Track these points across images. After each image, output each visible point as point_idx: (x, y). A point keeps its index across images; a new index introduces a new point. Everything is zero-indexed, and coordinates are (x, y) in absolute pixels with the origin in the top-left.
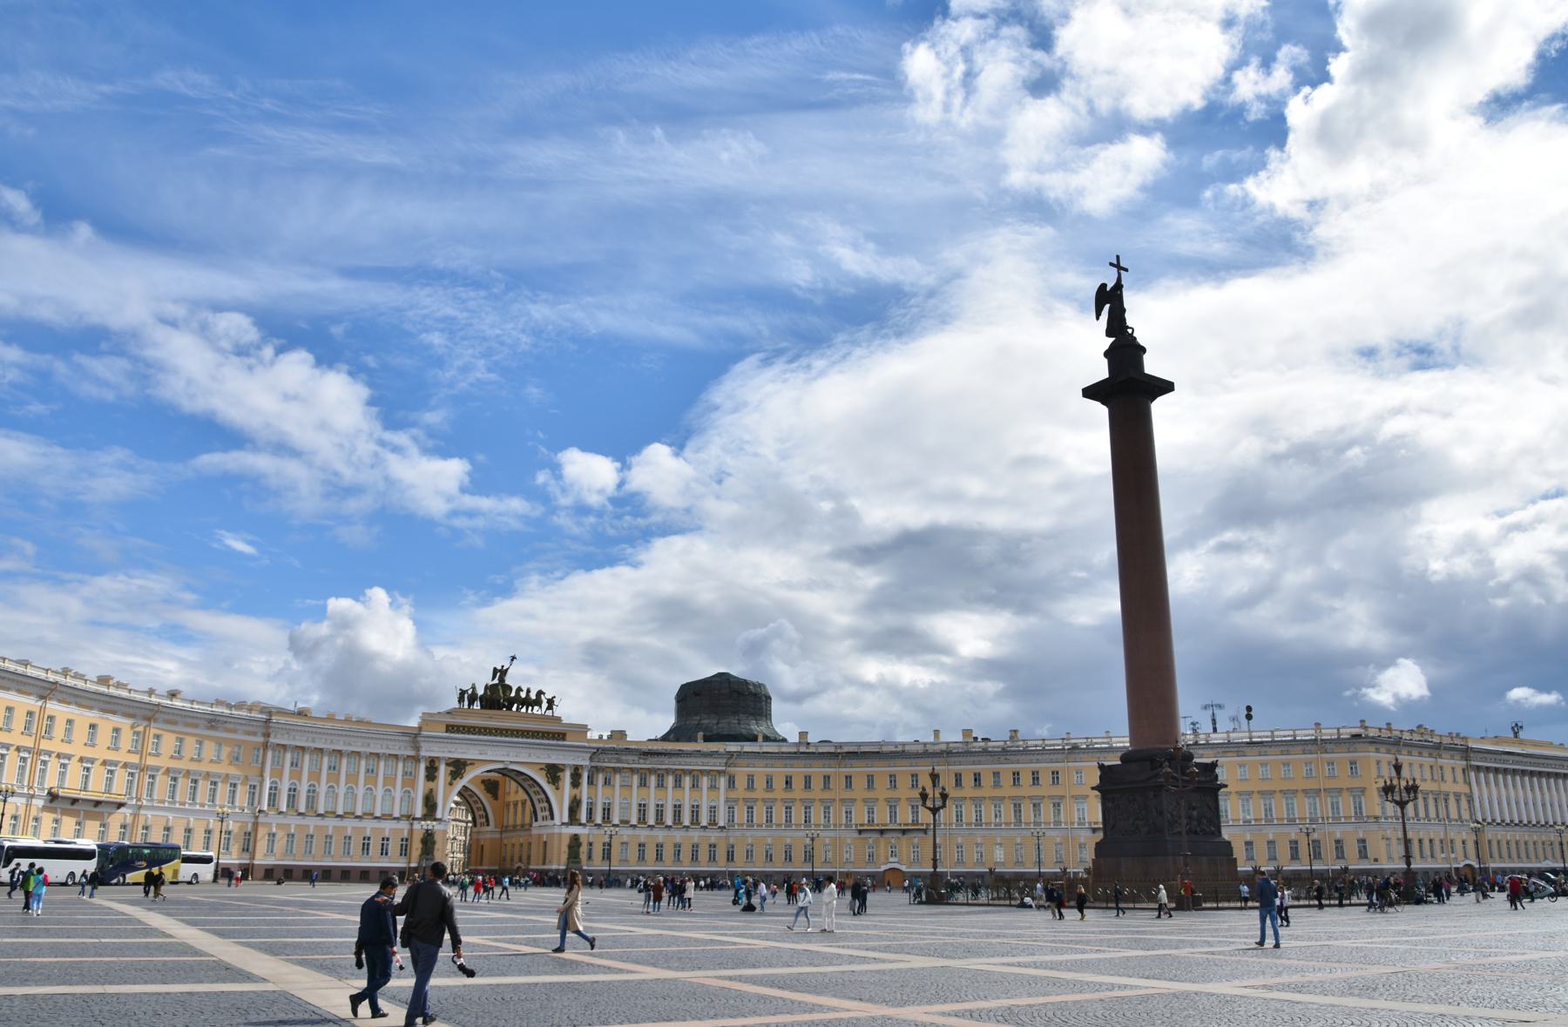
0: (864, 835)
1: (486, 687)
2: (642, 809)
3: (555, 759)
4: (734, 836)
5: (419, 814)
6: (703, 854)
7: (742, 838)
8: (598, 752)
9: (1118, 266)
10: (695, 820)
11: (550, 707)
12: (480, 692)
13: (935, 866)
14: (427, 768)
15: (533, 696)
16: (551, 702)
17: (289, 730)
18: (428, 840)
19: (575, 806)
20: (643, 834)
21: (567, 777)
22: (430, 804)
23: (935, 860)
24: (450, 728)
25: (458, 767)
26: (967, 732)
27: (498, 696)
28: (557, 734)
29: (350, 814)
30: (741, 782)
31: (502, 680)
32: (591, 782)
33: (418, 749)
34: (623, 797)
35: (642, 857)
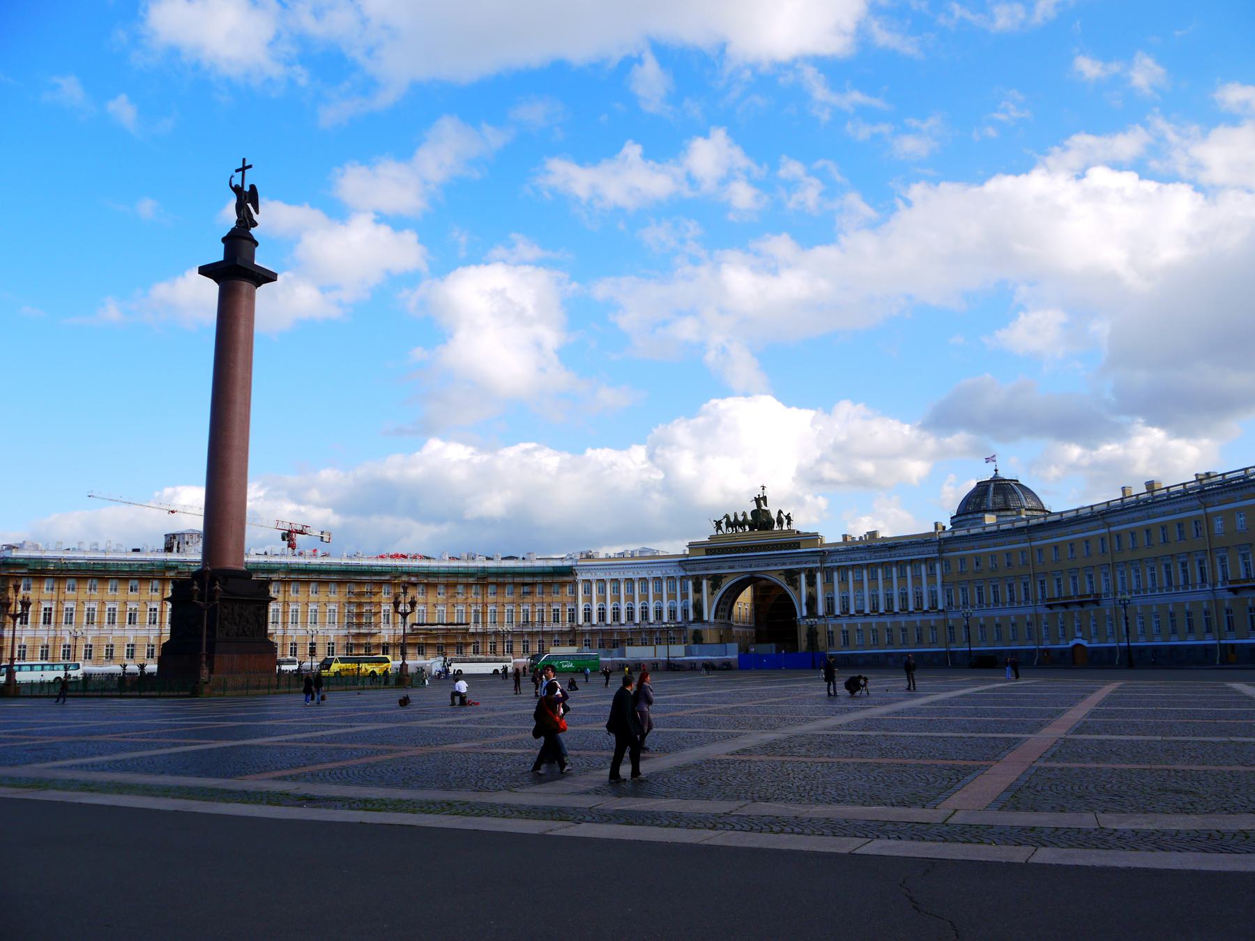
0: (1056, 610)
1: (753, 513)
4: (953, 617)
8: (826, 554)
10: (919, 607)
11: (789, 523)
16: (788, 517)
24: (709, 551)
26: (1150, 485)
28: (796, 541)
30: (956, 566)
32: (829, 581)
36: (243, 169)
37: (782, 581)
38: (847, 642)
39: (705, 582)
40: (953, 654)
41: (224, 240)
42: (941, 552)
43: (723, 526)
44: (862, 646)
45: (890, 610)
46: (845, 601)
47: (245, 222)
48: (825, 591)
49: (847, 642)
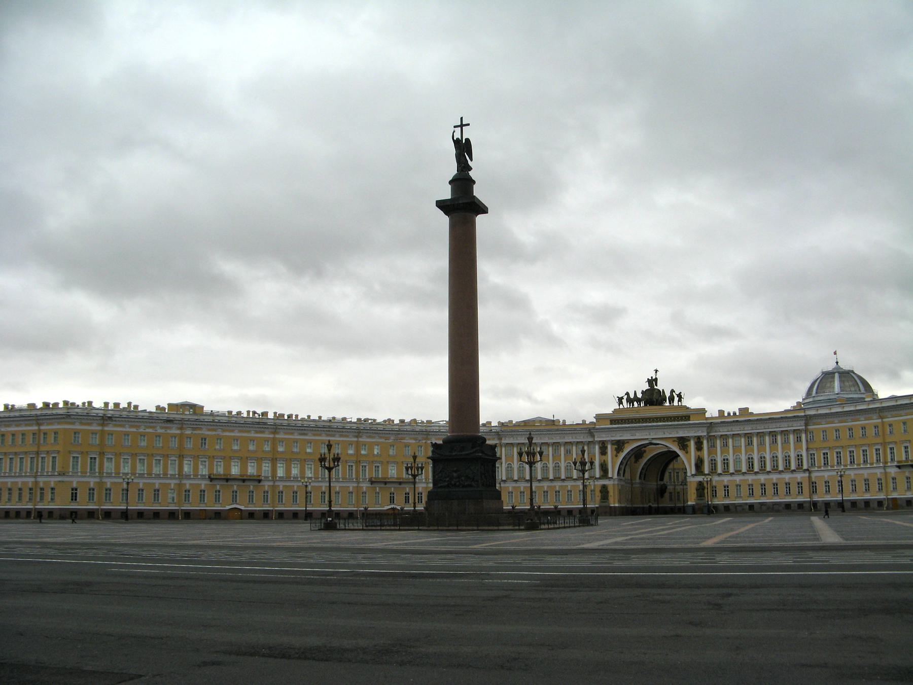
0: (903, 470)
3: (681, 434)
5: (598, 476)
6: (794, 489)
7: (822, 475)
8: (711, 425)
11: (680, 400)
12: (639, 395)
13: (330, 506)
14: (600, 448)
15: (668, 394)
16: (679, 396)
18: (604, 490)
20: (750, 478)
21: (692, 444)
22: (604, 468)
23: (330, 502)
24: (613, 421)
27: (653, 396)
28: (685, 416)
29: (557, 479)
33: (593, 436)
34: (736, 454)
35: (752, 494)
36: (462, 126)
37: (675, 448)
38: (727, 495)
39: (609, 447)
40: (815, 504)
41: (450, 182)
42: (806, 425)
43: (624, 401)
44: (739, 496)
45: (763, 469)
46: (726, 462)
48: (709, 453)
49: (727, 495)
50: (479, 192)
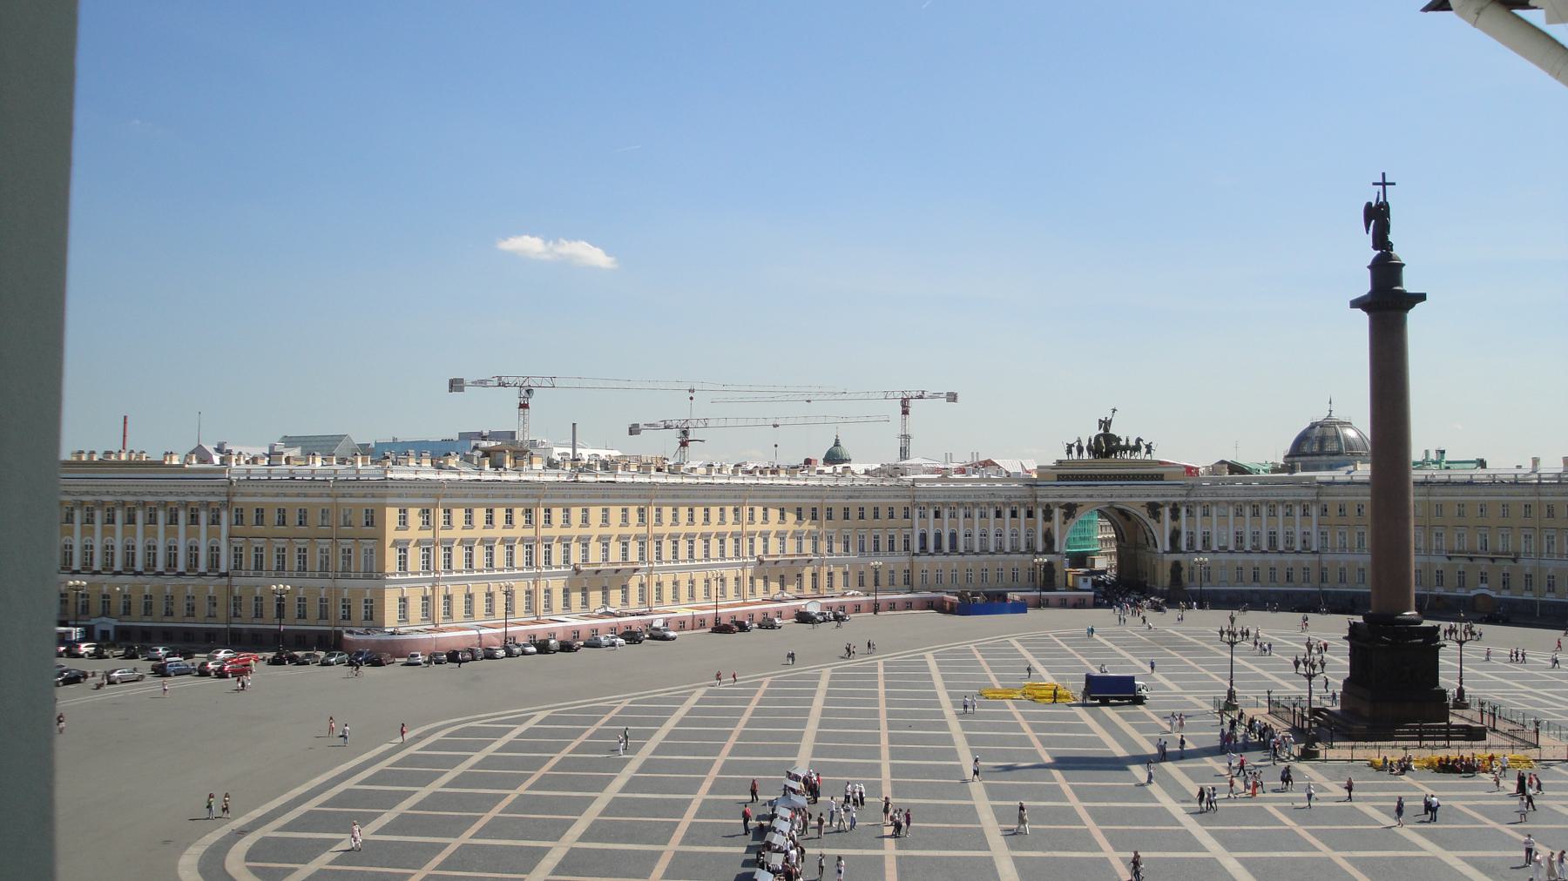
0: (1454, 561)
1: (1097, 438)
2: (1239, 538)
4: (1327, 558)
5: (1040, 549)
9: (1384, 184)
11: (1149, 452)
15: (1132, 443)
16: (1149, 447)
17: (924, 489)
19: (1175, 536)
20: (1240, 558)
21: (1166, 512)
24: (1061, 477)
25: (1070, 510)
27: (1106, 445)
28: (1155, 474)
30: (1333, 511)
31: (1106, 430)
40: (1325, 594)
43: (1074, 450)
47: (1381, 240)
50: (1409, 285)
